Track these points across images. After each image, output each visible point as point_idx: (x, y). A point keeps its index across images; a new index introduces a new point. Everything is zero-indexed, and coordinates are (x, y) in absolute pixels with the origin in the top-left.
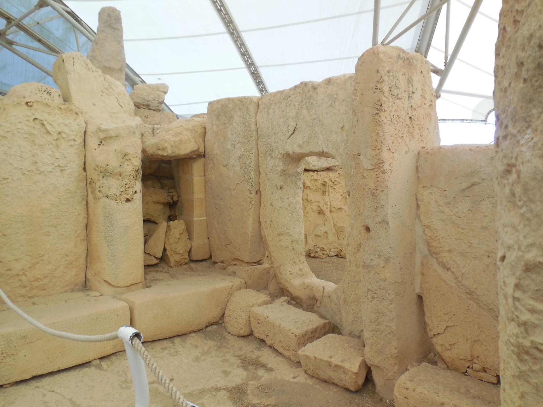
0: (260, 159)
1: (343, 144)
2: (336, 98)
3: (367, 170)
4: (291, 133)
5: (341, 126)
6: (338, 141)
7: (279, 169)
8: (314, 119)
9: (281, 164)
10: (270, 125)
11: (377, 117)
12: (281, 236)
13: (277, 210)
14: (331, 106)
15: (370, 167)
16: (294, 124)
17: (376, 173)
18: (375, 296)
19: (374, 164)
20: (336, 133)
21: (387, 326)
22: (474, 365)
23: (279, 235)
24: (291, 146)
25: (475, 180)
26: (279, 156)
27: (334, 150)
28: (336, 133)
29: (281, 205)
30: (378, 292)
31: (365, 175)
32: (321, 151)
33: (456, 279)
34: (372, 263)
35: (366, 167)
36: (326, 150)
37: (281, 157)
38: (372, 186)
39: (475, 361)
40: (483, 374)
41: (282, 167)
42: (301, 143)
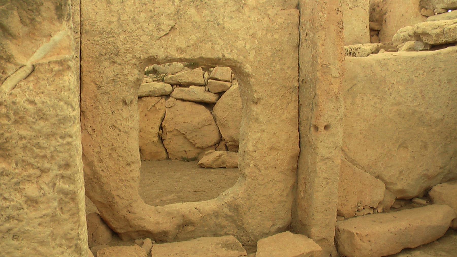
0: (84, 65)
1: (254, 51)
2: (245, 4)
3: (334, 77)
4: (162, 33)
5: (251, 32)
6: (247, 48)
7: (131, 78)
8: (208, 21)
9: (136, 72)
10: (115, 19)
11: (340, 34)
12: (132, 165)
13: (126, 133)
14: (238, 10)
15: (338, 75)
16: (172, 23)
17: (340, 80)
18: (329, 181)
19: (341, 73)
20: (244, 39)
21: (335, 202)
22: (359, 208)
23: (128, 165)
24: (163, 50)
25: (355, 82)
26: (134, 61)
27: (242, 57)
28: (244, 39)
29: (131, 125)
30: (331, 178)
31: (332, 82)
32: (221, 56)
33: (345, 154)
34: (330, 155)
35: (334, 75)
36: (227, 56)
37: (137, 63)
38: (336, 91)
39: (359, 205)
40: (364, 211)
41: (137, 76)
42: (184, 46)
